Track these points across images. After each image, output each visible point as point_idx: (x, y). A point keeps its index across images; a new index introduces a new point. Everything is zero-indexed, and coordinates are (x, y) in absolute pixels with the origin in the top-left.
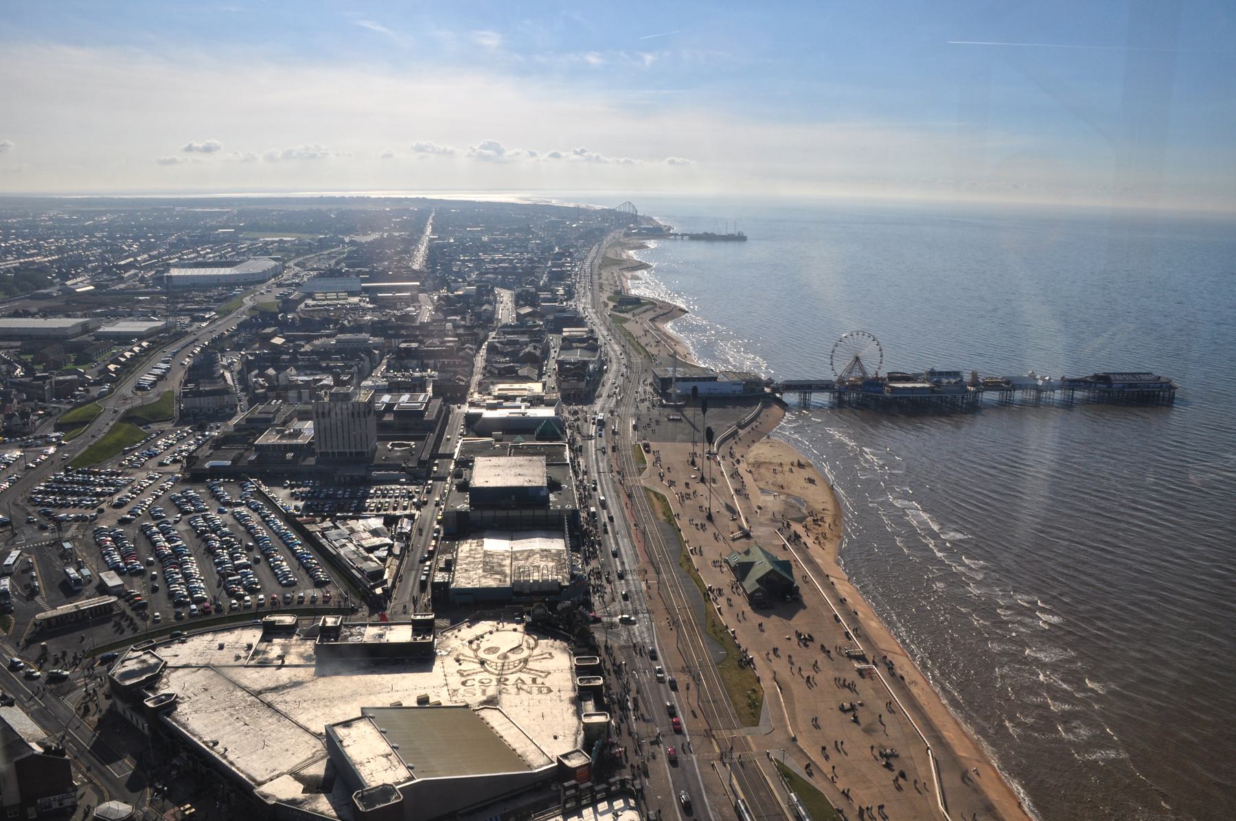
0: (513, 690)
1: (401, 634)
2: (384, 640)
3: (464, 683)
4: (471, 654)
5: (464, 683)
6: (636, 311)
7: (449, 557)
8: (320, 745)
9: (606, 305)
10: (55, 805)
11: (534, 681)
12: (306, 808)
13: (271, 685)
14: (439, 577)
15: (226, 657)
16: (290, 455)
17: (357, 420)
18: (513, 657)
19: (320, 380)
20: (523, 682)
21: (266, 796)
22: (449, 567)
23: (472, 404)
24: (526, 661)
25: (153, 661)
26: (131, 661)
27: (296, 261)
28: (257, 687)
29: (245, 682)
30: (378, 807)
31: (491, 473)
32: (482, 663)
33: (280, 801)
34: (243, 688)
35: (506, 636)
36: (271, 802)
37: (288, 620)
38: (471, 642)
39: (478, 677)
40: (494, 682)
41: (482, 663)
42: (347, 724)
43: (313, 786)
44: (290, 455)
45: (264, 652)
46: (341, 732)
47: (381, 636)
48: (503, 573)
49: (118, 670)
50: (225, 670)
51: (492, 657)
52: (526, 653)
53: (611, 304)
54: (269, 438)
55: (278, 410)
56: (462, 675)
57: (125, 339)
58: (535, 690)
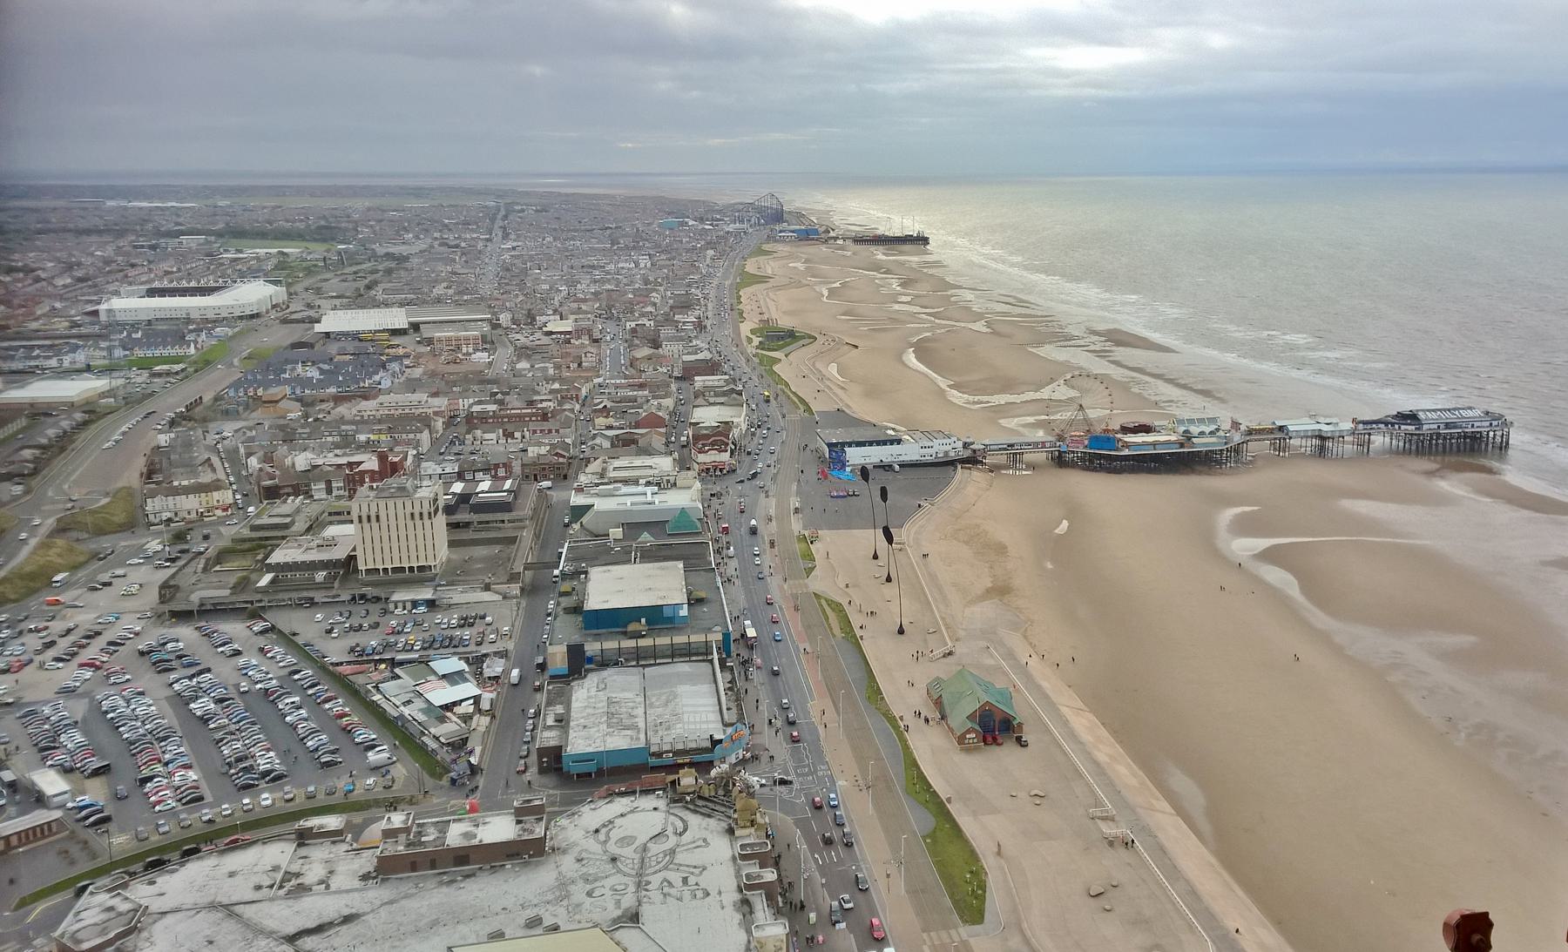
0: (656, 896)
1: (499, 829)
2: (475, 842)
3: (589, 894)
4: (597, 848)
5: (589, 894)
6: (788, 349)
7: (560, 709)
9: (750, 340)
11: (685, 880)
13: (311, 924)
14: (549, 738)
15: (239, 890)
16: (320, 576)
17: (419, 523)
18: (654, 848)
20: (670, 884)
22: (562, 722)
23: (580, 490)
24: (673, 852)
25: (124, 907)
28: (291, 930)
29: (270, 924)
31: (609, 588)
34: (270, 934)
35: (640, 817)
37: (332, 822)
38: (597, 831)
39: (609, 882)
40: (632, 888)
44: (320, 576)
45: (298, 875)
47: (467, 835)
48: (635, 727)
50: (238, 909)
52: (673, 840)
53: (756, 341)
55: (298, 511)
57: (39, 413)
58: (687, 895)
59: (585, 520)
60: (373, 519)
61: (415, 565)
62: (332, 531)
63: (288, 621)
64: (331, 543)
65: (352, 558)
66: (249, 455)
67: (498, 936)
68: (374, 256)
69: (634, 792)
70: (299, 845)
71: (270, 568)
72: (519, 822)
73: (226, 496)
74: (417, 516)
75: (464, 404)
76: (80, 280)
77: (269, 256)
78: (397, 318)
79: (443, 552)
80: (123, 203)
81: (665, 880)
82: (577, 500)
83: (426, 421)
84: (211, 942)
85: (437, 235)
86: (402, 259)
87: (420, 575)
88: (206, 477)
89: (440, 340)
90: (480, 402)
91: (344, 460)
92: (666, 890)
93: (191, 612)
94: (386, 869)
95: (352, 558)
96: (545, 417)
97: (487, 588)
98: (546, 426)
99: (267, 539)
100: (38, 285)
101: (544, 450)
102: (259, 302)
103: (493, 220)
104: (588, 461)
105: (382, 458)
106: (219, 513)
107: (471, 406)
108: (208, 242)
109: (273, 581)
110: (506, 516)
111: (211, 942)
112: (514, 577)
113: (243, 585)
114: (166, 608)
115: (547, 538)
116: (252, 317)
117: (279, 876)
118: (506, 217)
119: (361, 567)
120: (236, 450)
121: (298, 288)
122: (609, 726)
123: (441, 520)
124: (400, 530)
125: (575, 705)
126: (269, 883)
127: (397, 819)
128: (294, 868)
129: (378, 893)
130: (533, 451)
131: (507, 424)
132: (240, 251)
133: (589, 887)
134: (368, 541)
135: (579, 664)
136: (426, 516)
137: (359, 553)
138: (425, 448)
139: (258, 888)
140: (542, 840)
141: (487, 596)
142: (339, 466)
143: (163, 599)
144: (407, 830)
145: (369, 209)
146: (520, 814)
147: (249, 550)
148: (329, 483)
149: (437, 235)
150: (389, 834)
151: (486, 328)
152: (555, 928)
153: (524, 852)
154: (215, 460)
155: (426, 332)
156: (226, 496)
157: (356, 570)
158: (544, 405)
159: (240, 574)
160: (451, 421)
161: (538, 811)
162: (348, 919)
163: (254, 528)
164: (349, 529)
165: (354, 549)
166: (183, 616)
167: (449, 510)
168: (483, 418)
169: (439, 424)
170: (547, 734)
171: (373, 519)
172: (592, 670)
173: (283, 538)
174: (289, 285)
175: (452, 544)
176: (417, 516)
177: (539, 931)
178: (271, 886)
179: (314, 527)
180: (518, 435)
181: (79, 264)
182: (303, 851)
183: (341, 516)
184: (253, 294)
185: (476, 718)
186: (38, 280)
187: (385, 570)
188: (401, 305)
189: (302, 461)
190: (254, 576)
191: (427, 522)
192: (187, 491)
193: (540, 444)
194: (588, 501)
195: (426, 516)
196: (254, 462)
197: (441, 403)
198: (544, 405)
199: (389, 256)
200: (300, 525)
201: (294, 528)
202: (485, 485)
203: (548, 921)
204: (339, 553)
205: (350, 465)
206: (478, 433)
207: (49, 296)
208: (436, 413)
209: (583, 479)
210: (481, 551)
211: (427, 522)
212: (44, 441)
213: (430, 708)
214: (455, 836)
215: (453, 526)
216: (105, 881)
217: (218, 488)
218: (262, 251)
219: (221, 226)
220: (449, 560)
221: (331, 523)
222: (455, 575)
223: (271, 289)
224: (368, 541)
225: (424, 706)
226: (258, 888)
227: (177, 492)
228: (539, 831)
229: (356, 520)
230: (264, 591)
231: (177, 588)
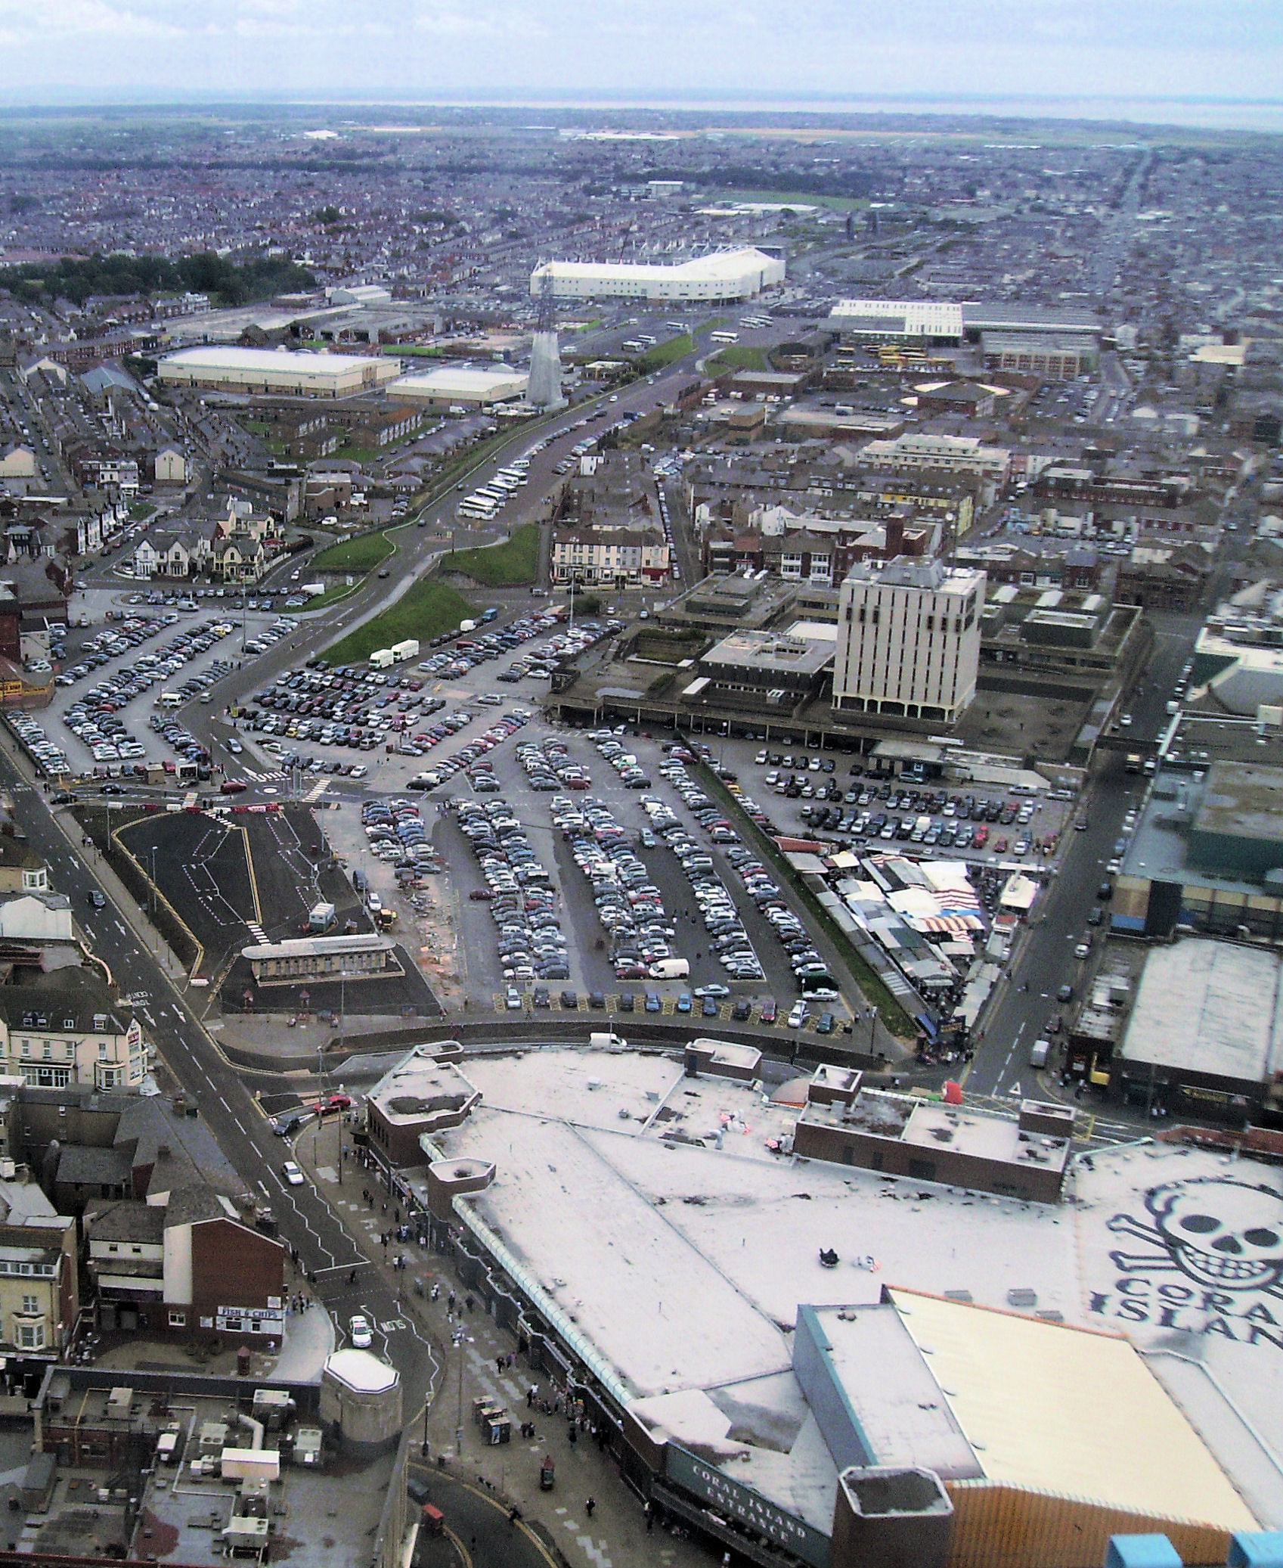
1: (988, 1137)
3: (1122, 1286)
4: (1149, 1220)
5: (1122, 1286)
7: (1121, 984)
8: (779, 1351)
10: (247, 1327)
12: (733, 1470)
14: (1096, 1026)
15: (600, 1111)
16: (776, 693)
17: (938, 636)
18: (1253, 1252)
19: (856, 535)
21: (650, 1425)
22: (1121, 1007)
23: (1216, 631)
25: (450, 1086)
26: (417, 1074)
27: (816, 258)
28: (661, 1192)
29: (634, 1172)
30: (894, 1513)
32: (1173, 1244)
33: (677, 1440)
34: (632, 1185)
36: (658, 1438)
37: (744, 1056)
39: (1159, 1278)
40: (1197, 1300)
41: (1173, 1244)
42: (845, 1315)
43: (758, 1432)
44: (776, 693)
45: (680, 1117)
46: (829, 1324)
47: (943, 1135)
48: (1249, 1047)
49: (382, 1095)
50: (592, 1136)
51: (1201, 1241)
54: (732, 650)
55: (758, 592)
56: (1120, 1266)
57: (435, 409)
59: (1217, 682)
60: (869, 617)
61: (920, 704)
62: (802, 630)
63: (723, 756)
64: (796, 649)
65: (824, 678)
66: (699, 501)
67: (961, 1298)
68: (923, 221)
69: (1228, 1151)
70: (687, 1075)
71: (703, 670)
72: (1023, 1138)
73: (658, 556)
74: (937, 624)
75: (1035, 464)
76: (514, 236)
77: (767, 215)
78: (944, 319)
79: (967, 693)
80: (582, 135)
81: (1261, 1307)
82: (1207, 644)
83: (968, 483)
84: (553, 1170)
85: (1030, 193)
86: (969, 228)
87: (926, 721)
88: (638, 525)
89: (1010, 359)
90: (1061, 464)
91: (833, 527)
92: (1260, 1323)
93: (590, 713)
94: (810, 1144)
95: (824, 678)
96: (1170, 499)
97: (1028, 764)
98: (1173, 516)
99: (707, 626)
100: (460, 241)
101: (1160, 557)
102: (743, 281)
103: (1128, 173)
104: (1237, 586)
105: (894, 529)
106: (646, 580)
107: (1047, 468)
108: (685, 192)
109: (705, 691)
110: (1078, 652)
111: (553, 1170)
112: (1076, 755)
113: (665, 687)
114: (560, 701)
115: (1147, 700)
116: (731, 302)
117: (655, 1109)
118: (1147, 172)
119: (838, 692)
120: (681, 493)
121: (802, 265)
122: (1199, 1033)
123: (972, 639)
124: (905, 633)
125: (1147, 983)
126: (642, 1115)
127: (835, 1077)
128: (675, 1106)
129: (786, 1177)
130: (1141, 556)
131: (1098, 498)
132: (729, 207)
133: (1124, 1275)
134: (855, 650)
135: (1165, 918)
136: (951, 626)
137: (838, 671)
138: (964, 525)
139: (625, 1116)
140: (1059, 1178)
141: (1031, 781)
142: (826, 535)
143: (557, 690)
144: (848, 1098)
145: (927, 151)
146: (1029, 1124)
147: (680, 638)
148: (806, 558)
149: (1030, 193)
150: (819, 1095)
151: (1090, 347)
152: (1054, 1319)
153: (1029, 1187)
154: (652, 503)
155: (993, 345)
156: (658, 556)
157: (828, 696)
158: (1174, 480)
159: (663, 672)
160: (1007, 492)
161: (1061, 1130)
162: (744, 1201)
163: (691, 607)
164: (828, 632)
165: (831, 663)
166: (574, 718)
167: (987, 627)
168: (1066, 487)
169: (990, 493)
170: (1089, 1016)
171: (869, 617)
172: (1188, 934)
173: (730, 629)
174: (790, 261)
175: (982, 684)
176: (937, 624)
177: (1030, 1312)
178: (643, 1121)
179: (777, 620)
180: (1118, 526)
181: (513, 214)
182: (692, 1085)
183: (818, 610)
184: (735, 268)
185: (975, 966)
186: (461, 232)
187: (873, 704)
188: (957, 298)
189: (772, 519)
190: (681, 679)
191: (952, 637)
192: (608, 540)
193: (1156, 546)
194: (1230, 650)
195: (951, 626)
196: (704, 513)
197: (998, 456)
198: (1174, 480)
199: (947, 225)
200: (761, 611)
201: (749, 617)
202: (1051, 596)
203: (1044, 1304)
204: (807, 665)
205: (844, 535)
206: (1052, 514)
207: (472, 256)
208: (987, 474)
209: (1224, 613)
210: (1026, 704)
211: (952, 637)
212: (439, 450)
213: (905, 933)
214: (919, 1130)
215: (987, 654)
216: (435, 1048)
217: (650, 543)
218: (758, 208)
219: (706, 168)
220: (973, 707)
221: (802, 618)
222: (977, 733)
223: (765, 262)
224: (855, 650)
225: (898, 925)
226: (625, 1116)
227: (593, 539)
228: (1055, 1162)
229: (842, 614)
230: (692, 702)
231: (576, 675)
